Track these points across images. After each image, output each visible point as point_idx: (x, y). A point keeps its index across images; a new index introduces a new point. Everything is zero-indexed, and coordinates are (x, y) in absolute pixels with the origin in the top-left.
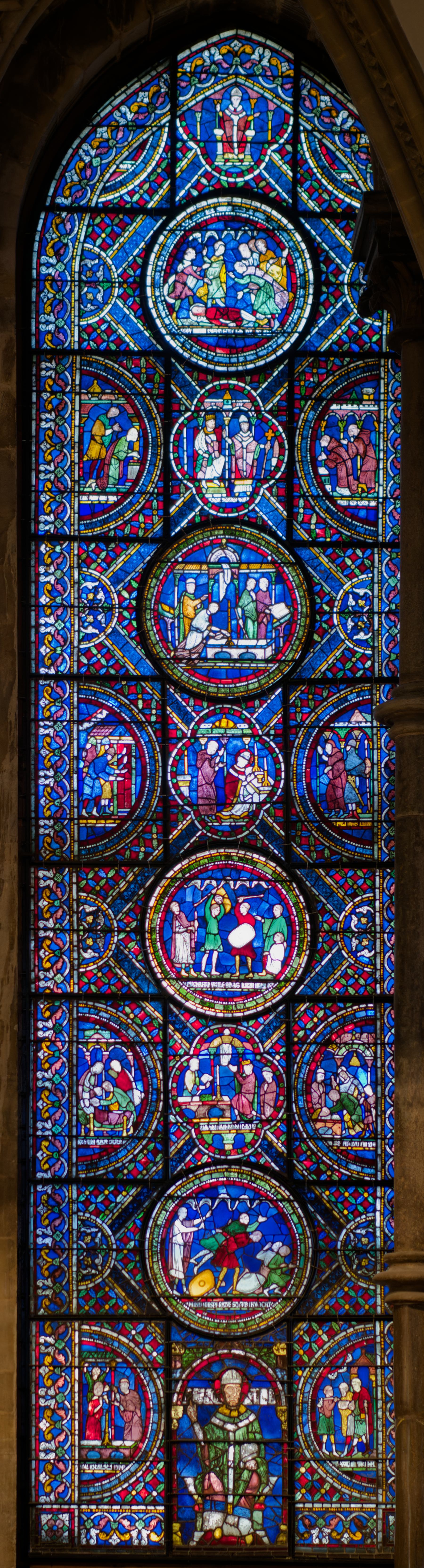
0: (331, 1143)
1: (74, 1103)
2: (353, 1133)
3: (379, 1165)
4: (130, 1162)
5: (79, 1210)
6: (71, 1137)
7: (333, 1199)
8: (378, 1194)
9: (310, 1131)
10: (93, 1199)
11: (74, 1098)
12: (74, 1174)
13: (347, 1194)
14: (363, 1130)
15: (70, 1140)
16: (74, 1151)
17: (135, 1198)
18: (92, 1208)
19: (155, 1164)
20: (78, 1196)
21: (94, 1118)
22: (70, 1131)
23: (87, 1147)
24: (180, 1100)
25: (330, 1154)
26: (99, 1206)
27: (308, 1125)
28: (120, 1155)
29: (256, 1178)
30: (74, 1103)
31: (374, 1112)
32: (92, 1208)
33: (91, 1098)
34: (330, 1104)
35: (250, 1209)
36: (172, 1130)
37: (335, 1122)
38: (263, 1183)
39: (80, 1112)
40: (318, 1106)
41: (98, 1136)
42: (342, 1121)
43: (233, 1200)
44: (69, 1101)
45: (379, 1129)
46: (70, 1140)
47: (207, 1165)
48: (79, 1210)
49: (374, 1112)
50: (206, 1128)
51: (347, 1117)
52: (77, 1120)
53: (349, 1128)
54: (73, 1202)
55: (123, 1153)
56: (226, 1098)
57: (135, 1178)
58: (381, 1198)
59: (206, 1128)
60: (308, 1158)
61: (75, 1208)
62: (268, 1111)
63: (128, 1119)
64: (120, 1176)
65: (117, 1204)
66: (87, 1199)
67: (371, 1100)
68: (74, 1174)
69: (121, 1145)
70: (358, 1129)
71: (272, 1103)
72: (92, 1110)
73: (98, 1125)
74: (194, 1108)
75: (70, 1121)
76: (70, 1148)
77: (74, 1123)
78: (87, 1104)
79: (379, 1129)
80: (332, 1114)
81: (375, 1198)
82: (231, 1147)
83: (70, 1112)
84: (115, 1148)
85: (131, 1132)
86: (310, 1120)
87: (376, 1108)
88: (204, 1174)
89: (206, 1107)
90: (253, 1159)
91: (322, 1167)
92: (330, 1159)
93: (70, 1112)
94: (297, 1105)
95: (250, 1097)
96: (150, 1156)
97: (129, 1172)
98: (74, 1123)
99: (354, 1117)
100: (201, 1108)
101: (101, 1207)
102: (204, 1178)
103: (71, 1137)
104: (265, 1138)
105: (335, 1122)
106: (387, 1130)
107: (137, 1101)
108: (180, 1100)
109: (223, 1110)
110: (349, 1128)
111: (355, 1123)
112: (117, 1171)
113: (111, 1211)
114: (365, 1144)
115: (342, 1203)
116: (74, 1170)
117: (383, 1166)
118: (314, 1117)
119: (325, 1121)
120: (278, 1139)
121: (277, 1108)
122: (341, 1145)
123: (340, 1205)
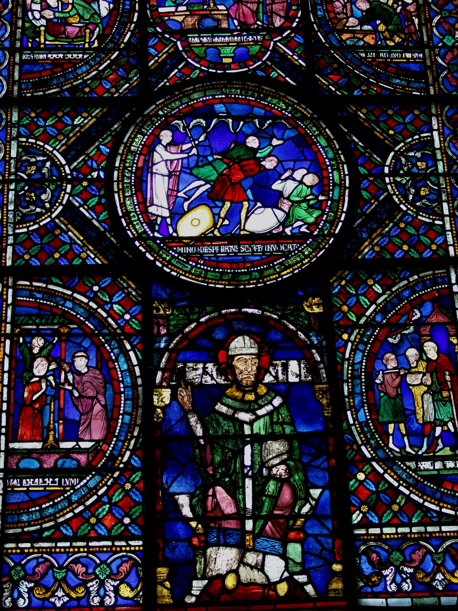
0: (363, 55)
1: (20, 14)
2: (392, 44)
3: (431, 79)
4: (93, 78)
5: (19, 135)
6: (12, 51)
7: (373, 118)
8: (433, 111)
9: (334, 42)
10: (41, 123)
11: (19, 10)
12: (16, 93)
13: (390, 112)
14: (403, 40)
15: (12, 55)
16: (17, 68)
17: (99, 119)
18: (38, 132)
19: (128, 80)
20: (20, 118)
21: (45, 31)
22: (13, 44)
23: (35, 62)
24: (161, 10)
25: (364, 68)
26: (49, 130)
27: (330, 36)
28: (79, 72)
29: (266, 96)
30: (20, 14)
31: (416, 21)
32: (38, 132)
33: (42, 10)
34: (359, 14)
35: (260, 130)
36: (151, 43)
37: (366, 33)
38: (275, 101)
39: (27, 25)
40: (342, 16)
41: (49, 49)
42: (375, 31)
43: (236, 119)
44: (13, 12)
45: (425, 39)
46: (12, 55)
47: (198, 80)
48: (19, 135)
49: (416, 21)
50: (197, 40)
51: (382, 28)
52: (23, 34)
53: (386, 39)
54: (13, 125)
55: (84, 69)
56: (221, 7)
57: (101, 97)
58: (437, 116)
59: (197, 40)
60: (336, 71)
61: (14, 132)
62: (278, 22)
63: (92, 32)
64: (78, 94)
65: (74, 127)
66: (32, 121)
67: (412, 8)
68: (16, 93)
69: (82, 60)
70: (397, 39)
71: (282, 14)
72: (43, 22)
73: (51, 38)
74: (180, 19)
75: (13, 33)
76: (12, 64)
77: (18, 36)
78: (37, 15)
79: (425, 39)
80: (361, 23)
81: (430, 115)
82: (230, 60)
83: (14, 25)
84: (74, 63)
85: (96, 45)
86: (333, 30)
87: (418, 16)
88: (195, 91)
89: (196, 18)
90: (260, 73)
91: (354, 81)
92: (364, 72)
93: (14, 25)
94: (315, 15)
95: (254, 7)
96: (121, 72)
97: (92, 90)
98: (18, 36)
99: (390, 27)
100: (189, 19)
101: (52, 131)
102: (195, 96)
103: (12, 51)
104: (275, 50)
105: (366, 33)
106: (436, 40)
107: (104, 13)
108: (161, 10)
109: (218, 20)
110: (386, 39)
111: (392, 34)
112: (73, 90)
113: (66, 136)
114: (409, 55)
115: (384, 122)
116: (16, 88)
117: (436, 79)
118: (339, 27)
119: (354, 32)
120: (293, 51)
121: (288, 18)
122: (378, 56)
123: (382, 125)
